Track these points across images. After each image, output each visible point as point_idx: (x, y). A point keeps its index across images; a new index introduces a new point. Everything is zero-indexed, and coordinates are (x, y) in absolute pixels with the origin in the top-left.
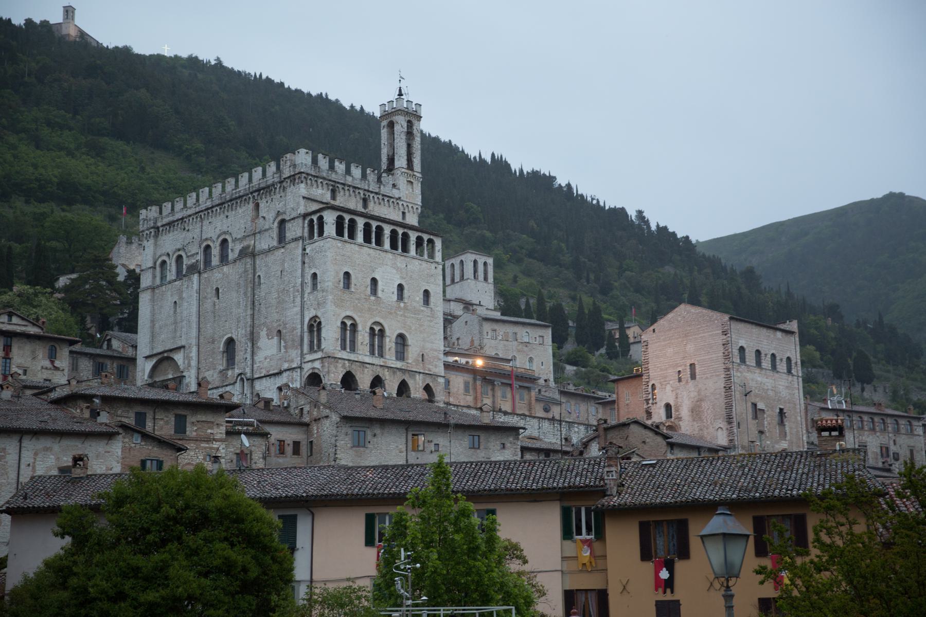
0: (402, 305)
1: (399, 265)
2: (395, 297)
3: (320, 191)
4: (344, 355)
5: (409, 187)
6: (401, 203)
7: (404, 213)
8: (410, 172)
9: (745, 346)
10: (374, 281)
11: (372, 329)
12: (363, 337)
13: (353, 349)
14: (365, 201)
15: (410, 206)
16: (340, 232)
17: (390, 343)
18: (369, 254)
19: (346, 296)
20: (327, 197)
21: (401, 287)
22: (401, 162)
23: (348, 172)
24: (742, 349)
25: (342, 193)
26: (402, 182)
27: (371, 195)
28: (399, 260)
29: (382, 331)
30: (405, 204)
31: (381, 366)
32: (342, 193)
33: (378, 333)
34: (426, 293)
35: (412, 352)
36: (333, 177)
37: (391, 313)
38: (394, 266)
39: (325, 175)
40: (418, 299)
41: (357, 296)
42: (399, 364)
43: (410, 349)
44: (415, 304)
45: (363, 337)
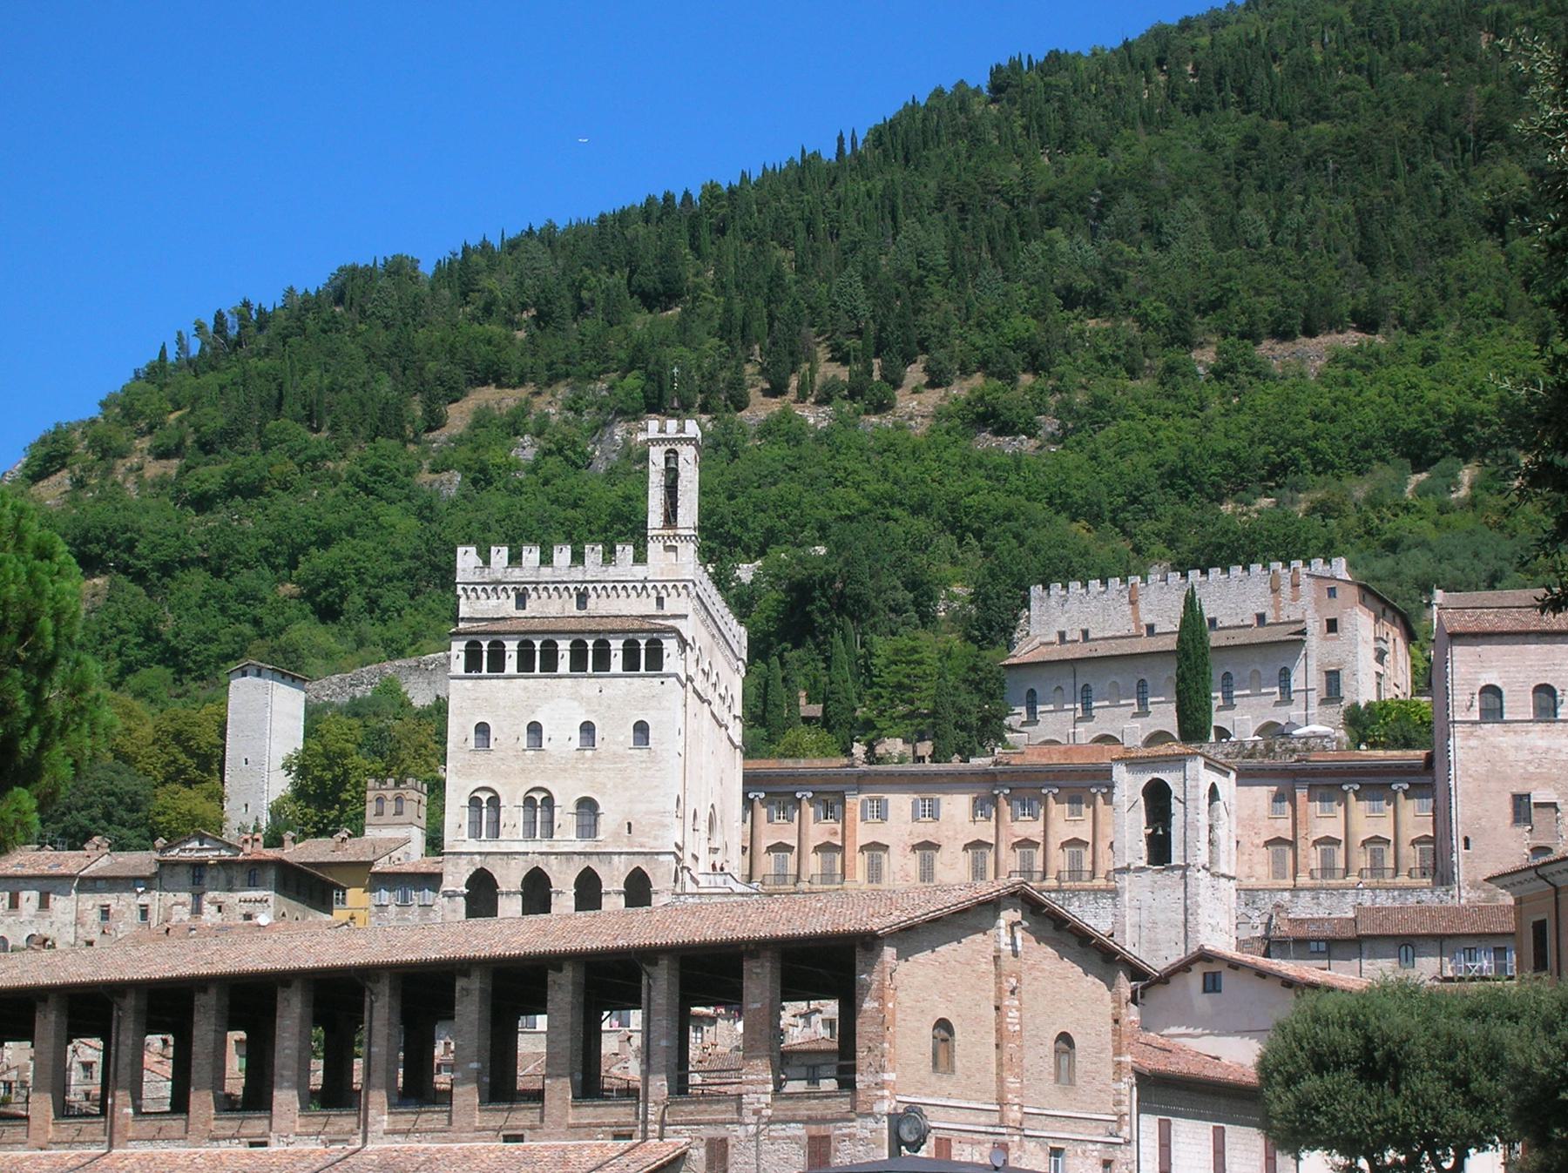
0: (589, 753)
1: (583, 692)
2: (576, 743)
3: (493, 601)
4: (473, 846)
5: (672, 555)
6: (649, 585)
7: (660, 601)
8: (671, 532)
9: (1499, 684)
10: (535, 729)
11: (529, 802)
12: (512, 815)
13: (495, 833)
14: (582, 599)
15: (670, 585)
16: (473, 663)
17: (565, 816)
18: (525, 688)
19: (481, 757)
20: (508, 606)
21: (587, 729)
22: (655, 519)
23: (546, 560)
24: (1492, 691)
25: (534, 595)
26: (654, 549)
27: (590, 587)
28: (589, 686)
29: (549, 802)
30: (659, 585)
31: (541, 854)
32: (534, 595)
33: (539, 805)
34: (641, 729)
35: (608, 821)
36: (516, 574)
37: (565, 770)
38: (576, 697)
39: (499, 576)
40: (621, 738)
41: (501, 755)
42: (580, 846)
43: (602, 819)
44: (615, 748)
45: (512, 815)
